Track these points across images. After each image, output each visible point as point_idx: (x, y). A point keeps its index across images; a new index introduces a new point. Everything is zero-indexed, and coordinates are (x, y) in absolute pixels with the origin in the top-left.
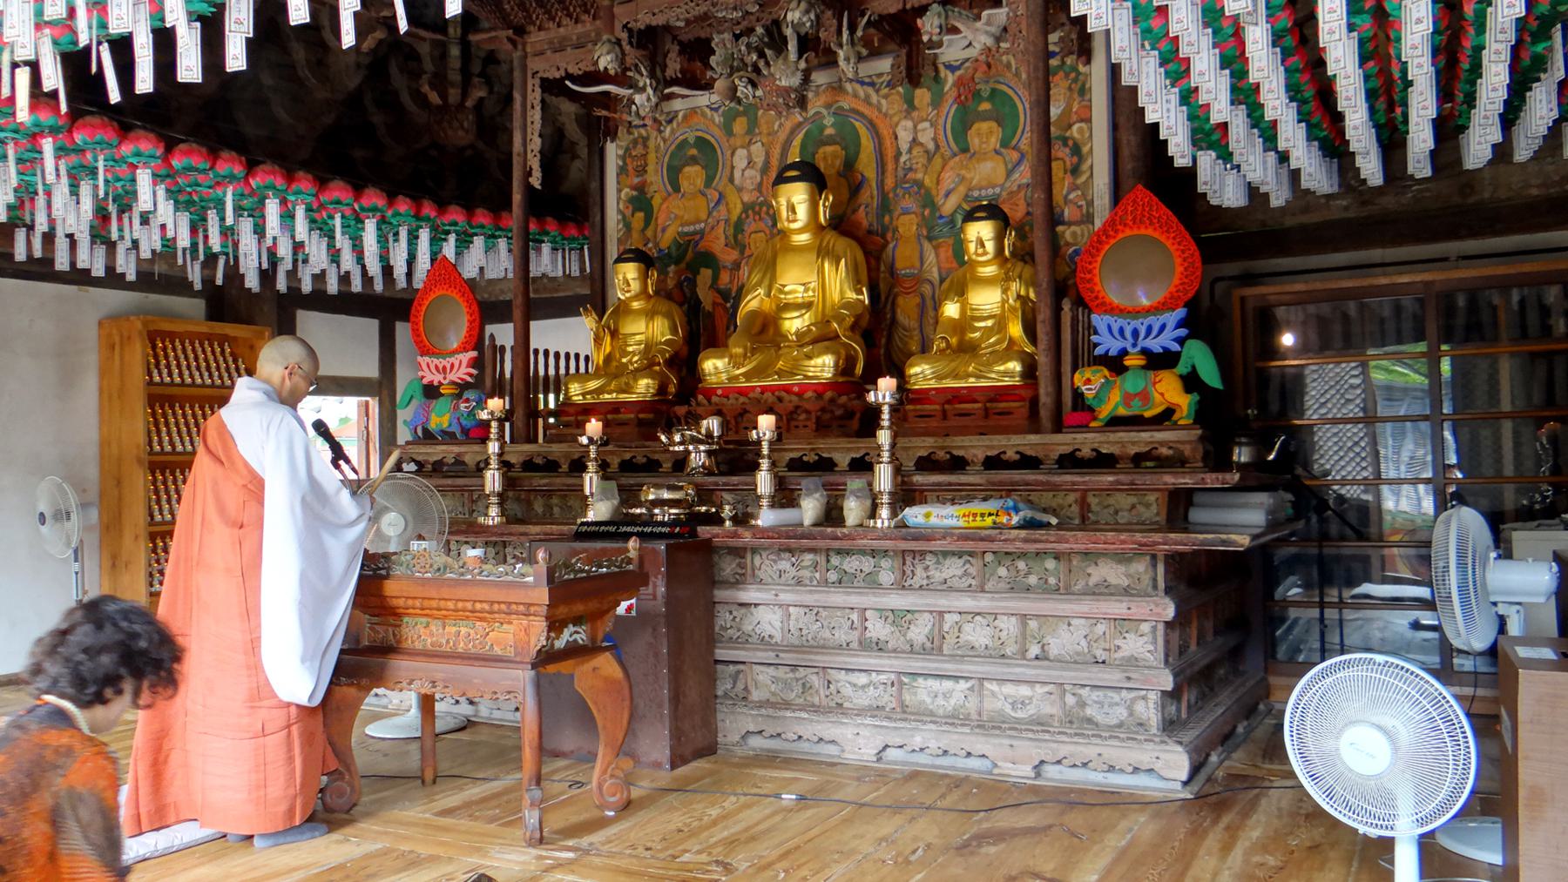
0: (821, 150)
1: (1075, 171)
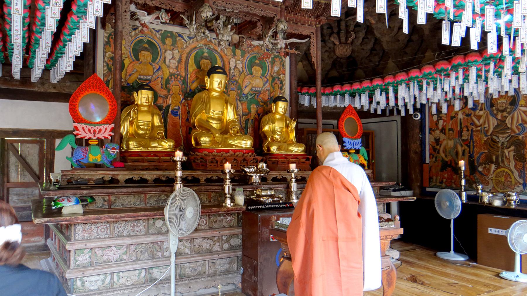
0: (203, 60)
1: (281, 88)
